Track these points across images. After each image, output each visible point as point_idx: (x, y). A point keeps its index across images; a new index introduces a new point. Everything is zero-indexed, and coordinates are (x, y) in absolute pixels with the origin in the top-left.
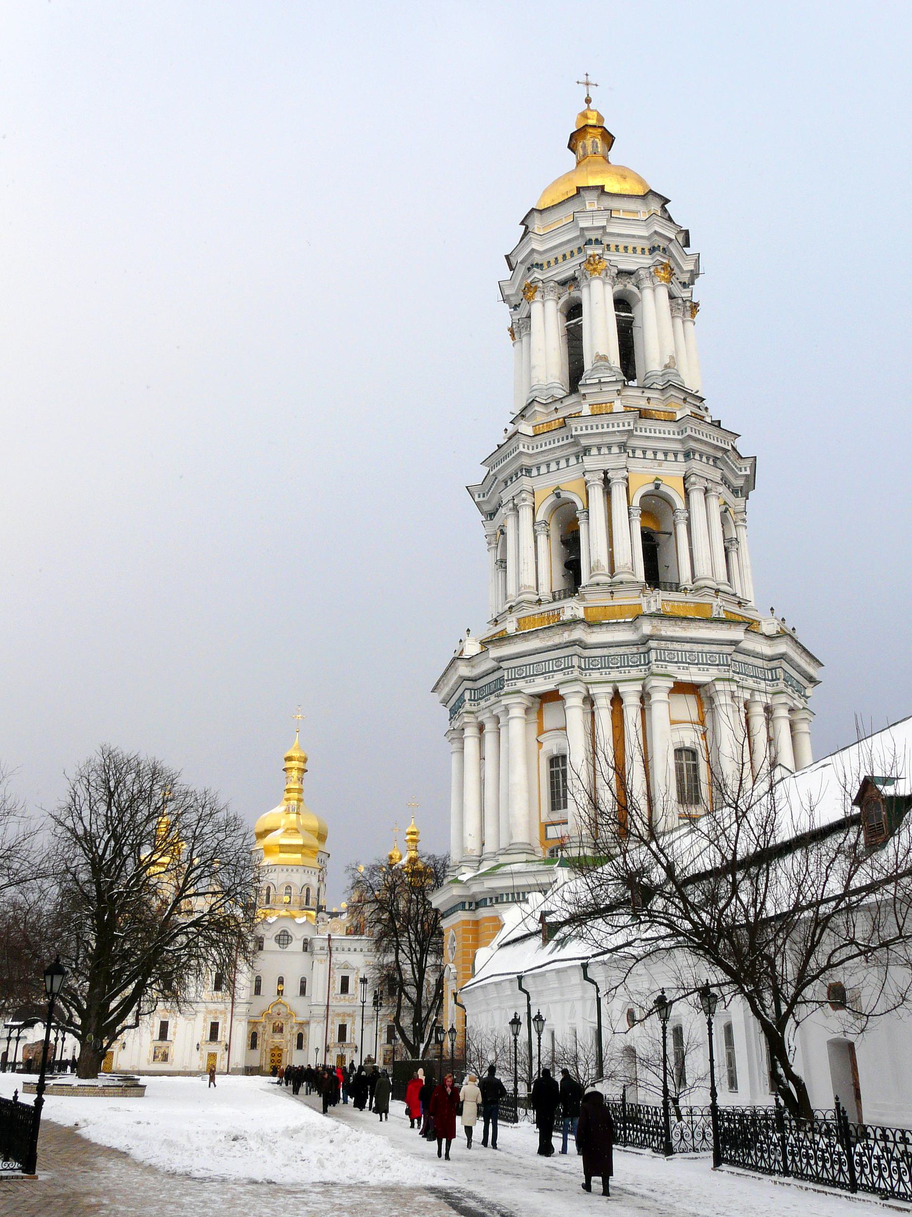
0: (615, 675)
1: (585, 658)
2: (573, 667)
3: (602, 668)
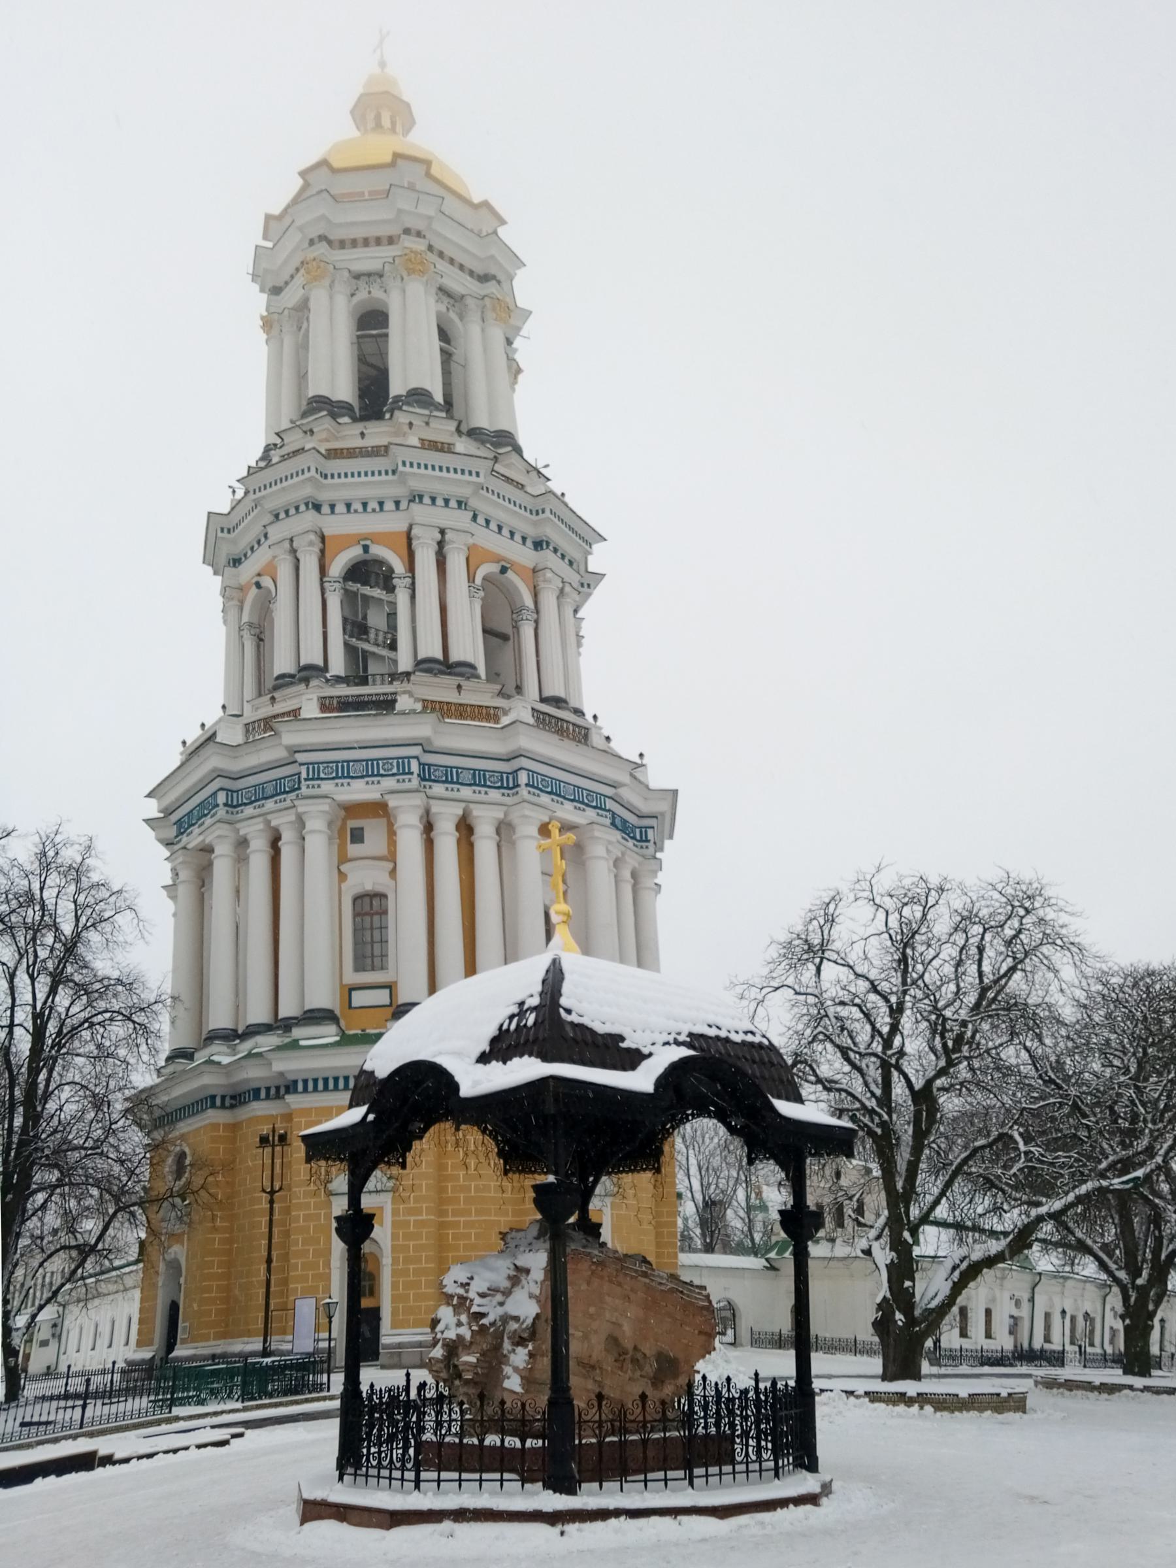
0: (270, 805)
1: (237, 791)
3: (256, 801)
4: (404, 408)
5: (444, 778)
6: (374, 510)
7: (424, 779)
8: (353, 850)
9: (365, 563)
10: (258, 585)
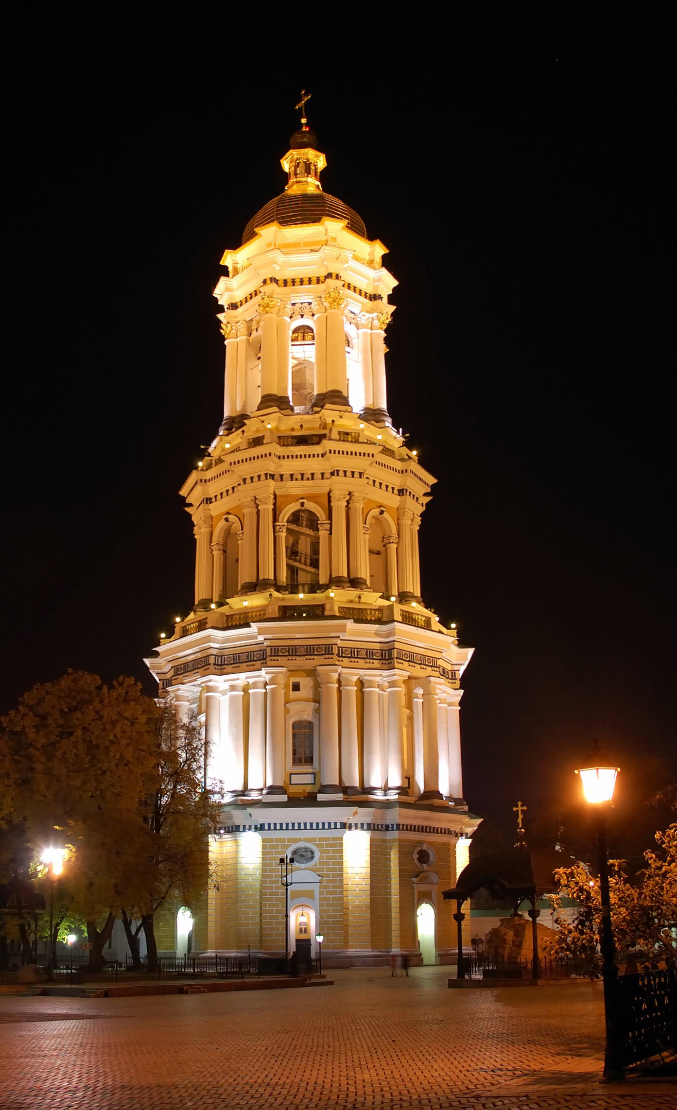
1: (221, 656)
2: (210, 664)
4: (327, 406)
5: (350, 655)
6: (308, 479)
7: (339, 657)
8: (293, 695)
9: (298, 511)
10: (227, 520)
